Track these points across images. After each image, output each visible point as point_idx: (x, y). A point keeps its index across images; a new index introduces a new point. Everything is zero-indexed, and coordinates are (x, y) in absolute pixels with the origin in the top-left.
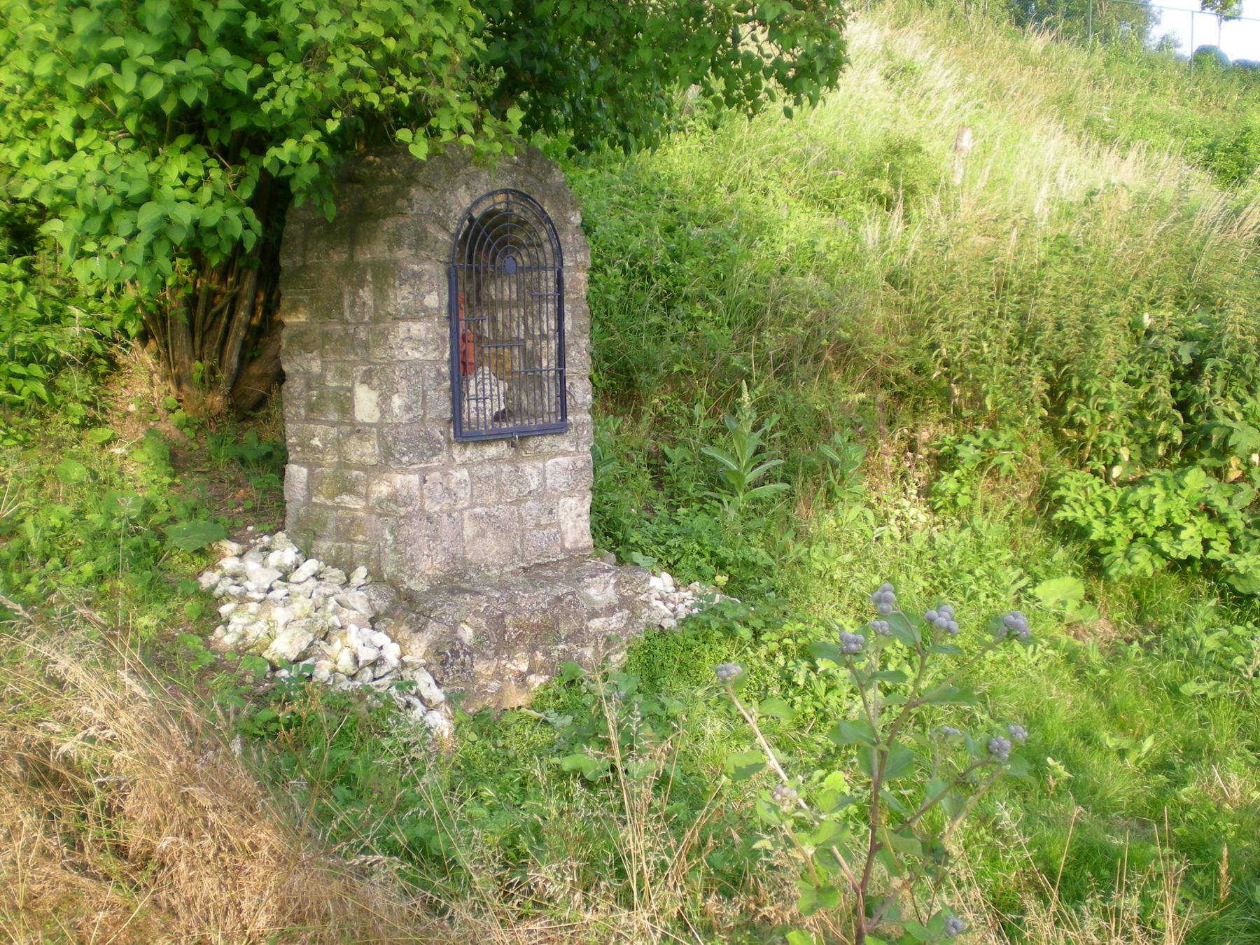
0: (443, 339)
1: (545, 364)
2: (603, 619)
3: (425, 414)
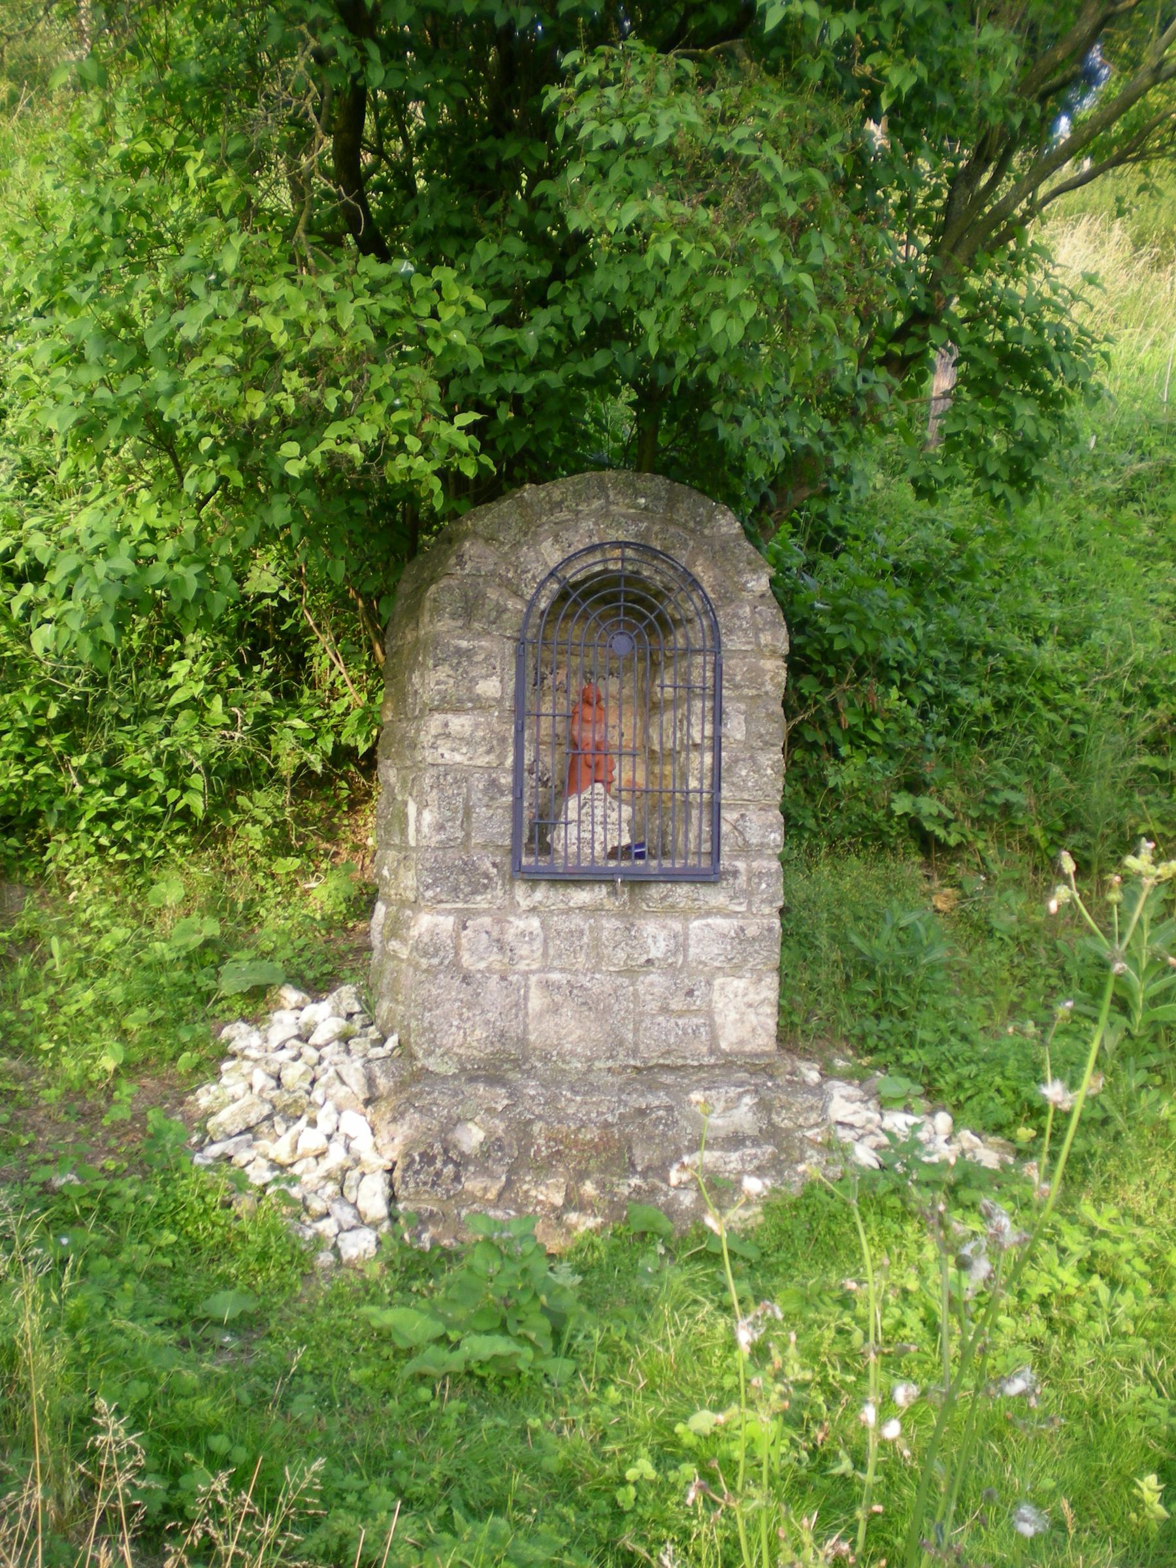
0: (503, 740)
1: (693, 784)
2: (717, 1154)
3: (468, 836)
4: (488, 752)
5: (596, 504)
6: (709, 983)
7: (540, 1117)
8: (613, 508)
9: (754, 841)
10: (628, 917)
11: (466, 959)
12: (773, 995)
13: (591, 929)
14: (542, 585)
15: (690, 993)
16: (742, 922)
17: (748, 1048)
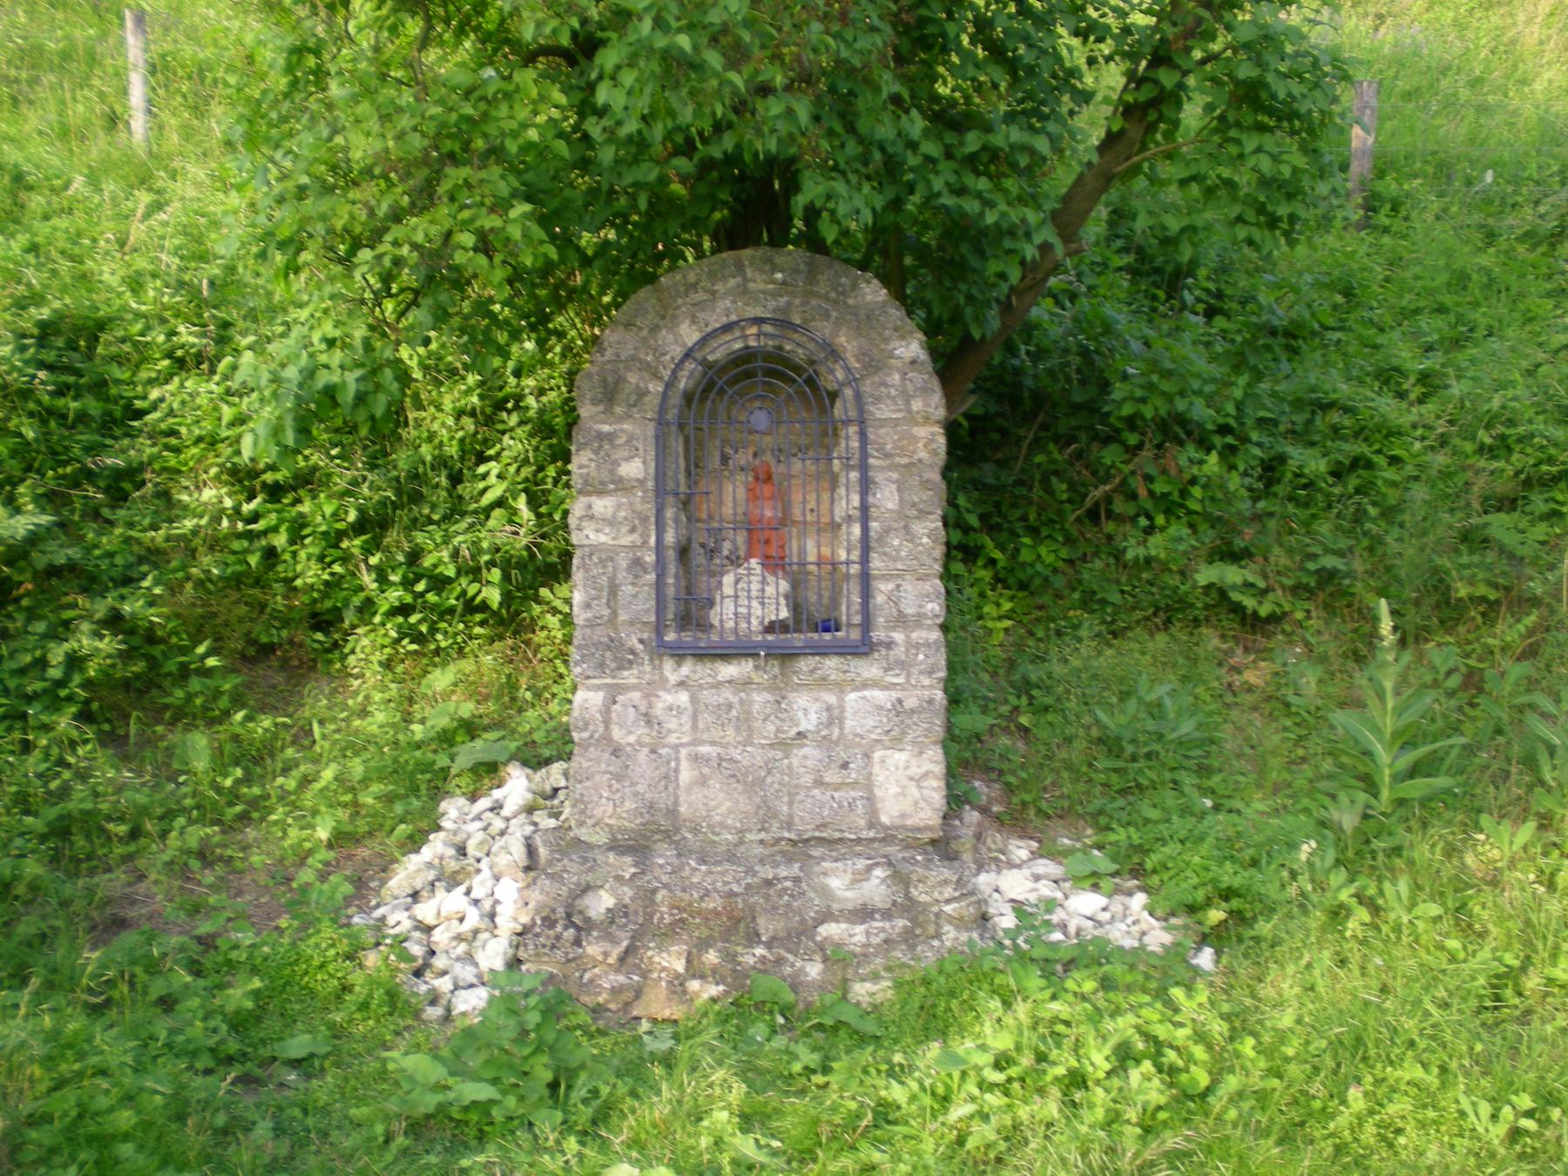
0: (645, 519)
2: (844, 926)
3: (614, 614)
4: (633, 530)
5: (732, 282)
6: (867, 756)
7: (666, 886)
8: (751, 285)
9: (910, 611)
10: (780, 691)
11: (617, 733)
12: (939, 769)
13: (741, 702)
14: (679, 366)
15: (845, 766)
16: (900, 694)
17: (909, 822)
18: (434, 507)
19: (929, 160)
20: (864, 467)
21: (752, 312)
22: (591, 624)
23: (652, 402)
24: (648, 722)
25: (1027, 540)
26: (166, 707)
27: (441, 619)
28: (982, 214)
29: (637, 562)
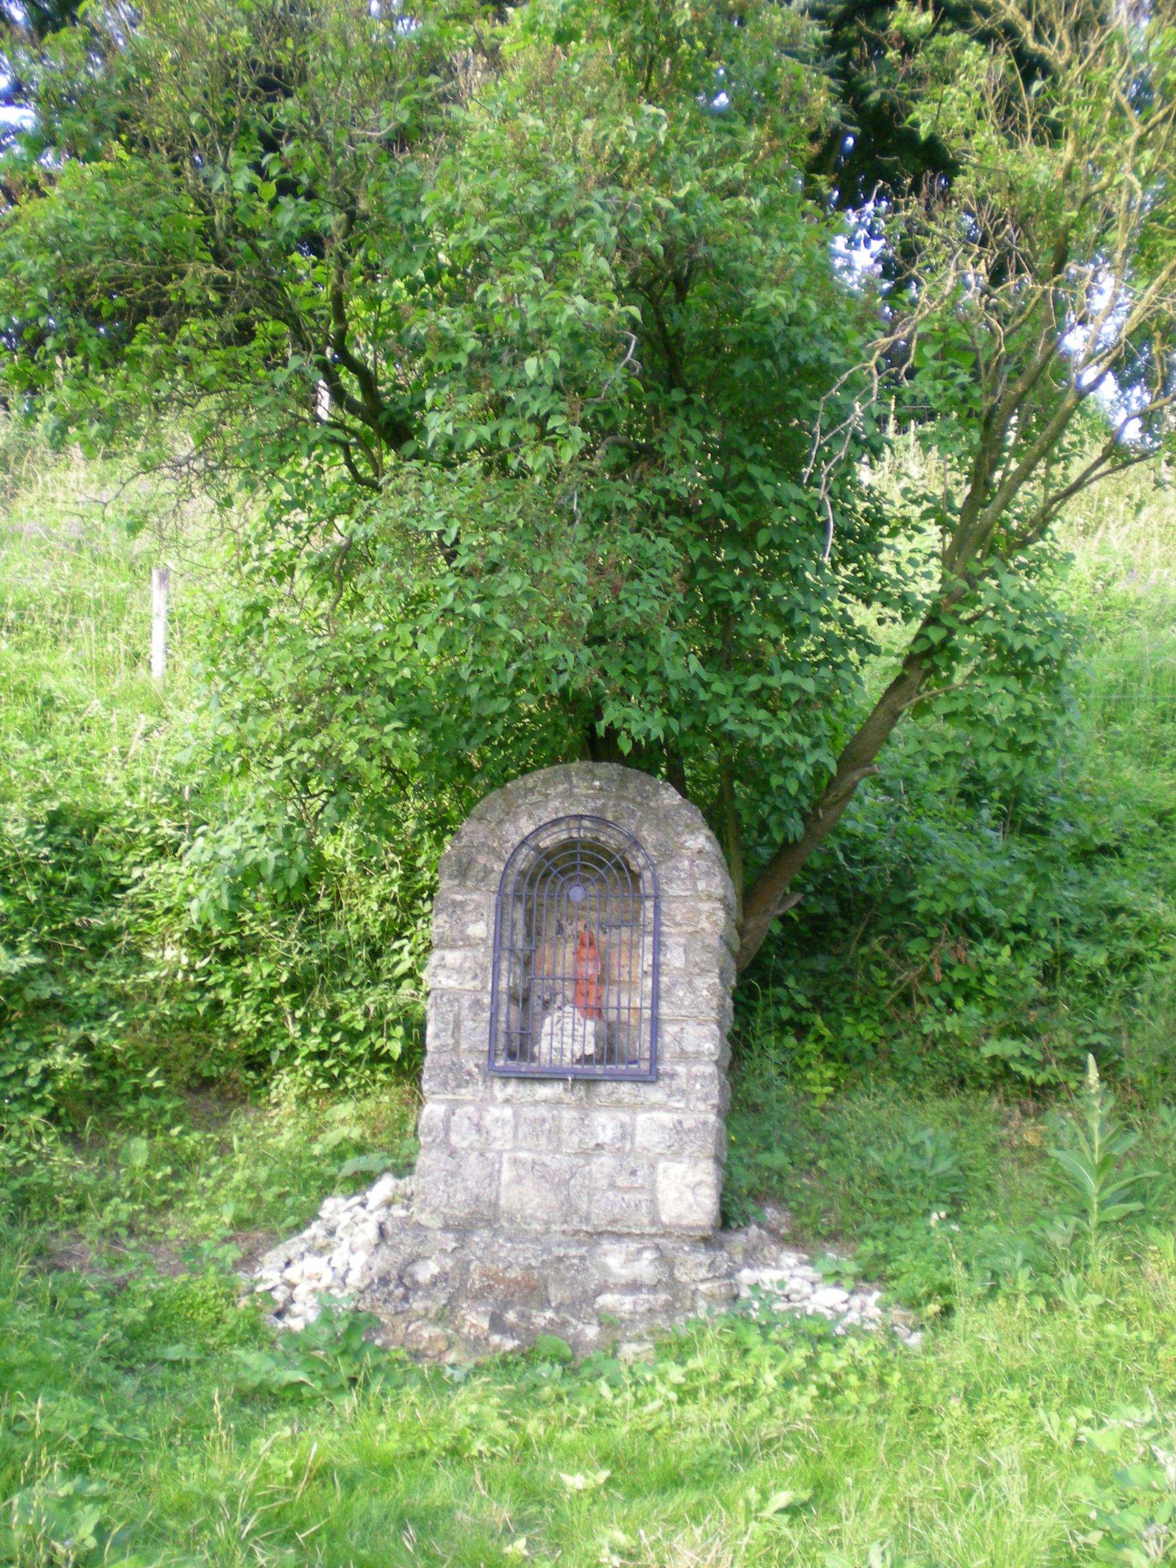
0: (485, 969)
3: (457, 1043)
4: (475, 977)
5: (561, 788)
6: (653, 1166)
9: (690, 1048)
10: (585, 1109)
11: (454, 1139)
14: (517, 850)
15: (633, 1173)
17: (684, 1222)
18: (355, 975)
19: (718, 697)
20: (657, 934)
21: (574, 811)
22: (439, 1051)
23: (495, 878)
24: (479, 1131)
25: (849, 1019)
26: (120, 1119)
27: (352, 1063)
28: (759, 738)
29: (477, 1003)
